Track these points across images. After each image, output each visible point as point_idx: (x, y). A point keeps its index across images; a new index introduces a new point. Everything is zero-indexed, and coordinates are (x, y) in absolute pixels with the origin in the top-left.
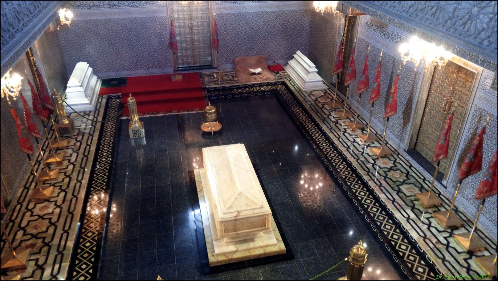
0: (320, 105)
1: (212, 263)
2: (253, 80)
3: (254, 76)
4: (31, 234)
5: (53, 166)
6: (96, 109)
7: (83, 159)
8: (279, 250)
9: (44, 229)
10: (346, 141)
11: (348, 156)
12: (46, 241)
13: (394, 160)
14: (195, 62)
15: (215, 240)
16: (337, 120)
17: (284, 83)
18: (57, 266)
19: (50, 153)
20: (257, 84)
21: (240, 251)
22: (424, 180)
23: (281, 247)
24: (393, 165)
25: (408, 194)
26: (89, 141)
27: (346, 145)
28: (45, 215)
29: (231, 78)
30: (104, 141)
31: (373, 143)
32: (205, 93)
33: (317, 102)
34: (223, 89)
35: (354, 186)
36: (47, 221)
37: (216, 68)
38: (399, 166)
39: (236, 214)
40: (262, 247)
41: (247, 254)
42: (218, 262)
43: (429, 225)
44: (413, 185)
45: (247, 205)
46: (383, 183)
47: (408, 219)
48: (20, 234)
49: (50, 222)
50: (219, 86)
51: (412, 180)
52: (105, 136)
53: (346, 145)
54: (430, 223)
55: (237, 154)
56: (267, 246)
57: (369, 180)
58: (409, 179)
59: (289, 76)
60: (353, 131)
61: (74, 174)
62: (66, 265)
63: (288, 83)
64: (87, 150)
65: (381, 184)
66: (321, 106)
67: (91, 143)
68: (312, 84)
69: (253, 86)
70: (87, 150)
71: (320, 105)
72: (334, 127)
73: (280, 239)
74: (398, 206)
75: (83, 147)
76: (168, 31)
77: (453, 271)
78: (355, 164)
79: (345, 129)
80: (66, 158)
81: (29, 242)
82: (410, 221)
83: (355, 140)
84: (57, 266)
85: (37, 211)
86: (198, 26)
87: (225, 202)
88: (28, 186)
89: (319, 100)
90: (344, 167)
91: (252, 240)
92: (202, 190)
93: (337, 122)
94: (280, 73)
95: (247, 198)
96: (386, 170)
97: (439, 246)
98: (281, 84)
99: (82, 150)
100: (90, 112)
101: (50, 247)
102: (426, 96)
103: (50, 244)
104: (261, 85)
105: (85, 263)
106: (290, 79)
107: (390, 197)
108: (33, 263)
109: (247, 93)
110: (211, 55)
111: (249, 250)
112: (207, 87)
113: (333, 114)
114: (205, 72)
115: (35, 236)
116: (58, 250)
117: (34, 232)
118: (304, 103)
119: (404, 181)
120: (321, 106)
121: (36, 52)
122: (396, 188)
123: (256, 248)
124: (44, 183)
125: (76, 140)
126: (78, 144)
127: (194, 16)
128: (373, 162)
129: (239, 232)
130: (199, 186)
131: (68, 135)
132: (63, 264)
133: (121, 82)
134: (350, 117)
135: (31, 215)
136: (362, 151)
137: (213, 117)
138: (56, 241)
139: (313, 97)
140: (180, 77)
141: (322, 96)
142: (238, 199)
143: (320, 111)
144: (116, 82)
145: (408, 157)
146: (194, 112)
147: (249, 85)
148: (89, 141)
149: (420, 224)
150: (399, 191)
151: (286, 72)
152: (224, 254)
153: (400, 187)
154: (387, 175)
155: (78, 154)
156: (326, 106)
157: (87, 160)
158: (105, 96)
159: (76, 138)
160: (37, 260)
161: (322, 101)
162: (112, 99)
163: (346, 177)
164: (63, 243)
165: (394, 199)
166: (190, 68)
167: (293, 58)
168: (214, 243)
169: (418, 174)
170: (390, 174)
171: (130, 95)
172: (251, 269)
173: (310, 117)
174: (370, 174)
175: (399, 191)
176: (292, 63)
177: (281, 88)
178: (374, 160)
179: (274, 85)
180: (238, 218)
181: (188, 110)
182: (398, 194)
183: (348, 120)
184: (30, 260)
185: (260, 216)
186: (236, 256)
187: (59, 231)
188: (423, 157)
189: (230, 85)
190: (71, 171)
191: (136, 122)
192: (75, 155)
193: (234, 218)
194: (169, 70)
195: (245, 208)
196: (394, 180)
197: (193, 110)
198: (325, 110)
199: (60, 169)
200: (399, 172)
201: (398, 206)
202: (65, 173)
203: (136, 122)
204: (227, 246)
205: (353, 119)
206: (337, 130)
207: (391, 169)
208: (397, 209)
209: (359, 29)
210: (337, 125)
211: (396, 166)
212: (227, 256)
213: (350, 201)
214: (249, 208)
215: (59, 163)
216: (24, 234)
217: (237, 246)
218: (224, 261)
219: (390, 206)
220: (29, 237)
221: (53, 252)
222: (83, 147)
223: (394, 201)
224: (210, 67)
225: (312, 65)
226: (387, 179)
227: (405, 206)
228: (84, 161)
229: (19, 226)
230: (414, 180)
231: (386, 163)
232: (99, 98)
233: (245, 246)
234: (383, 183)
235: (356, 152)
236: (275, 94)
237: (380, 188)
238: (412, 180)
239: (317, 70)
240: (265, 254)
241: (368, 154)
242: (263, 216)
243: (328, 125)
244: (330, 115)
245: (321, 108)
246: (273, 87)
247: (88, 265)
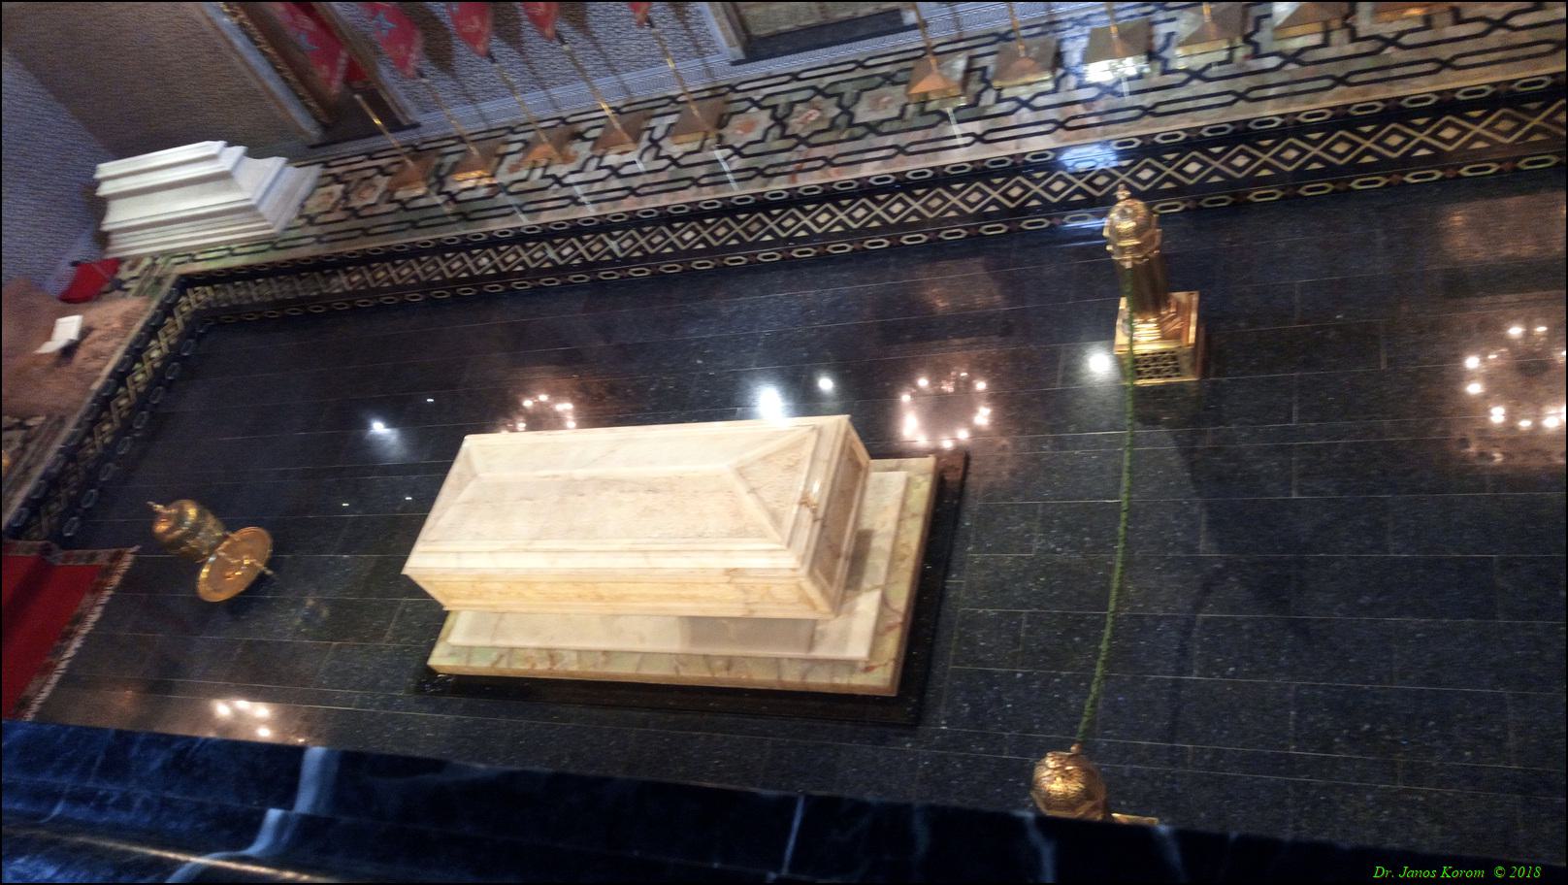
2: (94, 364)
3: (81, 355)
8: (930, 477)
10: (597, 187)
17: (187, 282)
20: (122, 362)
21: (887, 582)
22: (860, 65)
25: (895, 113)
31: (652, 129)
38: (782, 100)
39: (807, 513)
40: (900, 520)
44: (865, 95)
45: (792, 468)
47: (979, 138)
56: (904, 506)
57: (794, 181)
58: (840, 95)
60: (567, 160)
68: (274, 197)
69: (120, 376)
77: (1190, 104)
91: (863, 539)
92: (552, 655)
95: (766, 459)
96: (776, 131)
97: (1100, 106)
98: (182, 292)
104: (136, 353)
106: (190, 255)
111: (894, 558)
122: (858, 131)
130: (527, 660)
134: (502, 149)
137: (212, 526)
142: (754, 484)
146: (94, 617)
149: (1012, 120)
151: (138, 259)
152: (878, 634)
168: (821, 652)
174: (770, 171)
176: (118, 216)
177: (195, 299)
180: (820, 514)
183: (510, 160)
188: (788, 33)
189: (58, 445)
193: (818, 525)
197: (80, 619)
200: (799, 108)
204: (851, 612)
212: (890, 628)
213: (824, 259)
217: (866, 584)
219: (911, 165)
225: (213, 147)
227: (933, 133)
233: (878, 564)
235: (662, 176)
236: (209, 325)
238: (849, 90)
239: (239, 150)
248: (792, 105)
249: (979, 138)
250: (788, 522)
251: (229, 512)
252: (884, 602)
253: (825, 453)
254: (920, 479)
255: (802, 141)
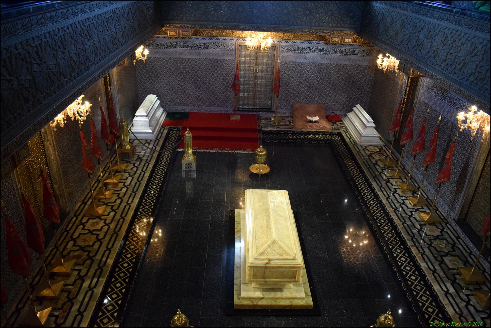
0: (374, 161)
1: (237, 305)
2: (308, 127)
3: (310, 124)
4: (80, 246)
5: (110, 187)
6: (157, 138)
7: (136, 183)
8: (306, 304)
9: (91, 243)
10: (395, 201)
11: (395, 218)
12: (91, 255)
13: (441, 228)
14: (255, 104)
15: (243, 283)
16: (388, 179)
17: (340, 135)
18: (95, 280)
19: (109, 174)
22: (470, 254)
23: (310, 301)
24: (440, 234)
25: (451, 267)
26: (145, 168)
27: (394, 206)
28: (94, 230)
29: (288, 123)
30: (158, 169)
31: (423, 208)
32: (260, 135)
33: (371, 158)
34: (278, 133)
35: (395, 250)
36: (95, 236)
37: (274, 112)
38: (446, 236)
39: (266, 261)
40: (289, 299)
41: (273, 303)
42: (243, 305)
43: (468, 303)
44: (457, 258)
45: (280, 254)
46: (427, 251)
47: (447, 293)
48: (71, 244)
49: (97, 238)
50: (276, 129)
51: (457, 252)
52: (160, 165)
53: (394, 206)
54: (469, 300)
55: (279, 200)
56: (294, 298)
58: (454, 251)
59: (346, 128)
60: (404, 192)
61: (126, 196)
62: (103, 280)
63: (344, 134)
64: (142, 176)
65: (424, 252)
66: (375, 162)
67: (146, 170)
68: (368, 139)
69: (309, 133)
70: (142, 176)
71: (374, 161)
72: (384, 185)
73: (309, 293)
74: (438, 278)
75: (138, 172)
76: (234, 73)
78: (400, 227)
79: (395, 189)
80: (122, 181)
81: (77, 253)
82: (448, 295)
83: (404, 202)
84: (95, 280)
85: (88, 226)
86: (262, 71)
87: (257, 248)
88: (85, 201)
89: (373, 155)
90: (389, 228)
91: (280, 290)
92: (239, 231)
93: (388, 181)
94: (338, 123)
95: (280, 247)
96: (432, 238)
98: (337, 135)
99: (137, 175)
100: (151, 140)
101: (93, 261)
102: (482, 166)
103: (93, 258)
104: (316, 133)
105: (120, 282)
106: (347, 131)
107: (431, 267)
108: (76, 273)
109: (301, 139)
110: (271, 99)
112: (263, 129)
113: (385, 172)
114: (263, 114)
115: (82, 248)
116: (99, 266)
117: (82, 244)
118: (357, 157)
119: (449, 252)
120: (375, 162)
121: (114, 82)
122: (439, 259)
123: (283, 299)
124: (99, 201)
125: (134, 165)
126: (135, 169)
127: (260, 61)
128: (419, 228)
129: (267, 280)
130: (237, 227)
131: (127, 160)
132: (100, 279)
133: (184, 116)
134: (402, 178)
135: (83, 229)
136: (410, 214)
137: (263, 159)
138: (99, 257)
139: (367, 152)
140: (238, 117)
141: (377, 152)
142: (271, 246)
143: (372, 167)
144: (179, 116)
145: (457, 227)
146: (245, 152)
147: (304, 132)
148: (145, 168)
149: (458, 301)
150: (442, 262)
151: (344, 124)
152: (250, 299)
153: (444, 258)
154: (432, 243)
155: (133, 178)
156: (379, 163)
157: (139, 185)
158: (167, 128)
159: (134, 164)
160: (80, 271)
161: (377, 157)
162: (173, 130)
163: (389, 239)
164: (104, 259)
165: (435, 270)
166: (249, 110)
167: (351, 110)
168: (242, 286)
169: (465, 247)
170: (435, 243)
171: (188, 129)
172: (274, 319)
173: (362, 172)
174: (414, 240)
175: (442, 262)
176: (351, 115)
177: (336, 138)
178: (420, 225)
179: (330, 135)
180: (268, 265)
181: (240, 150)
182: (440, 265)
183: (400, 180)
184: (74, 270)
185: (291, 267)
186: (261, 303)
187: (103, 248)
189: (286, 130)
190: (123, 194)
191: (189, 156)
192: (130, 179)
193: (264, 265)
194: (229, 110)
195: (277, 257)
196: (439, 249)
197: (245, 150)
198: (378, 167)
199: (115, 191)
200: (444, 241)
201: (438, 278)
202: (119, 194)
203: (189, 156)
204: (255, 291)
205: (405, 180)
206: (387, 189)
207: (436, 238)
208: (437, 281)
209: (421, 90)
210: (388, 184)
211: (442, 235)
212: (252, 302)
213: (390, 265)
214: (281, 257)
215: (115, 185)
216: (74, 245)
217: (264, 293)
218: (249, 306)
220: (78, 248)
221: (95, 267)
222: (138, 172)
223: (434, 272)
224: (269, 110)
225: (371, 120)
226: (431, 248)
227: (445, 279)
228: (137, 185)
229: (72, 237)
230: (460, 253)
231: (433, 231)
232: (161, 129)
233: (272, 295)
234: (427, 251)
235: (404, 215)
236: (330, 144)
237: (422, 255)
238: (457, 252)
239: (374, 125)
240: (291, 306)
241: (415, 218)
242: (294, 267)
243: (378, 182)
244: (382, 172)
245: (375, 164)
246: (328, 137)
247: (122, 284)
248: (445, 239)
249: (447, 293)
250: (262, 257)
251: (269, 162)
252: (262, 298)
253: (288, 262)
254: (304, 302)
255: (430, 246)
